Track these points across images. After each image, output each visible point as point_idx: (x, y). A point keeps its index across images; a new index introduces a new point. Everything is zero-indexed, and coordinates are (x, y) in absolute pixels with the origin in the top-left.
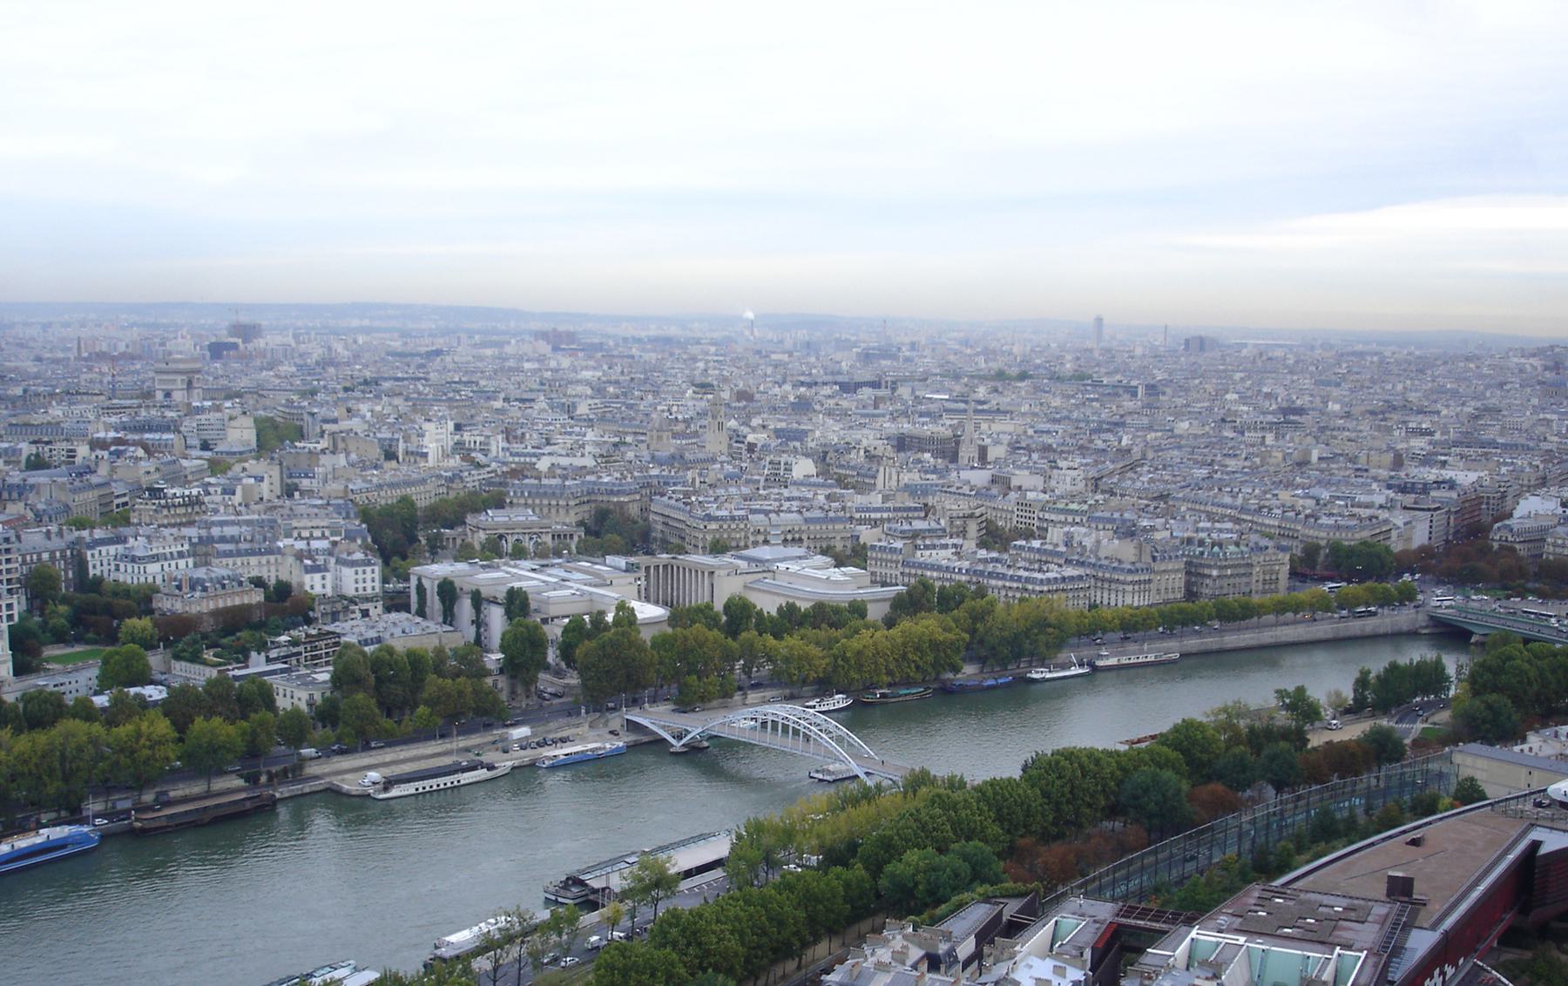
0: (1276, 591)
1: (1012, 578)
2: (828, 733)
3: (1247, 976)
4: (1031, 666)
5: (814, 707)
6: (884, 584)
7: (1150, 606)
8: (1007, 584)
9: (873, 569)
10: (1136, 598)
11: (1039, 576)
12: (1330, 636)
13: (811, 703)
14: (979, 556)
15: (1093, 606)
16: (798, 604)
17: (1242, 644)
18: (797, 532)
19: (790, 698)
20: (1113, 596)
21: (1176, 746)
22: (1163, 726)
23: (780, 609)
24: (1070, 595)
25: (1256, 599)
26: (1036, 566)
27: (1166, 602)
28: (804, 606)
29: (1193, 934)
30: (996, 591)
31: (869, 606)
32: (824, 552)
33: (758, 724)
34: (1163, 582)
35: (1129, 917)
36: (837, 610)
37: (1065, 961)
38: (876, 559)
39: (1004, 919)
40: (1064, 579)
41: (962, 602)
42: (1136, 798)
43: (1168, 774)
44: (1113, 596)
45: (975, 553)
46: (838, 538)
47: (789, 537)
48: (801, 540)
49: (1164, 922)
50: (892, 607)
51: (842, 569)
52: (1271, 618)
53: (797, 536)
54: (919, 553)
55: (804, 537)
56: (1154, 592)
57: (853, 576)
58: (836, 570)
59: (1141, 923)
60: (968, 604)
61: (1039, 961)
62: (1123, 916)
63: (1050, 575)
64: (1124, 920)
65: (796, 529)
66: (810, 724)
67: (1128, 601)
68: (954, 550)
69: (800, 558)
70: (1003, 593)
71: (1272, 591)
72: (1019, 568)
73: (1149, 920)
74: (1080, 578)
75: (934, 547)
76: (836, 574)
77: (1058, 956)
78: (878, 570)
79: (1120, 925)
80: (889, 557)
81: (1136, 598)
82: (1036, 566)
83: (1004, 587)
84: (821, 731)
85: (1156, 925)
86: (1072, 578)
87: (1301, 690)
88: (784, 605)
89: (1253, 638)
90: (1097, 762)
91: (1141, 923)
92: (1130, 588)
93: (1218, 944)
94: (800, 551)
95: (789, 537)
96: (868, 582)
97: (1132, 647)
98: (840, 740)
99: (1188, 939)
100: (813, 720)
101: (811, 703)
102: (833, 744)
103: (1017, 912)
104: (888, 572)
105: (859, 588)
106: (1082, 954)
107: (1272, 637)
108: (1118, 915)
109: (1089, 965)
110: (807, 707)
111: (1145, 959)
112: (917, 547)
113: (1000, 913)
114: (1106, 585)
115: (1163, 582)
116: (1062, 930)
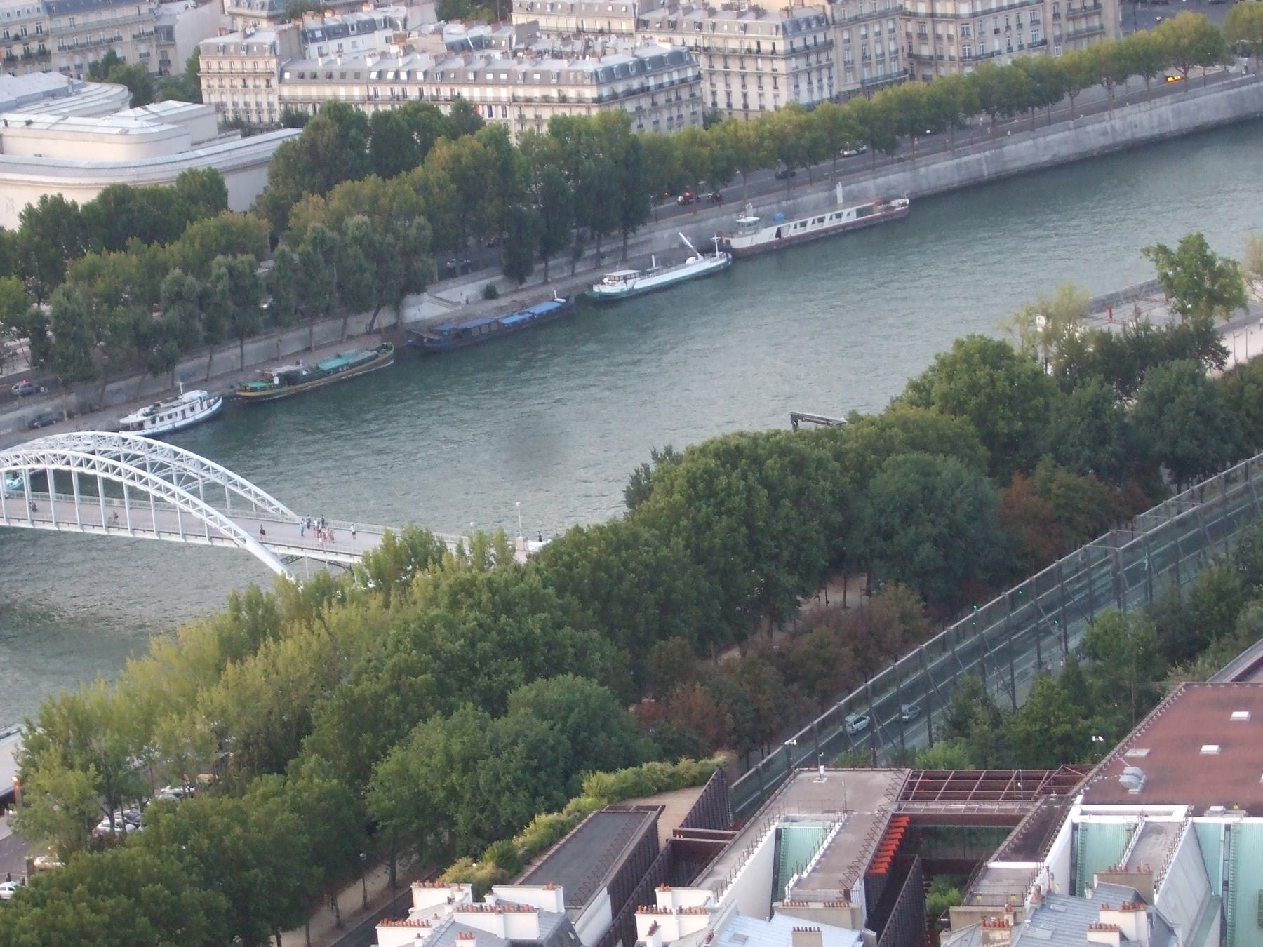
0: (1101, 31)
1: (526, 79)
2: (185, 479)
3: (1200, 889)
4: (598, 267)
5: (140, 426)
6: (248, 130)
7: (837, 99)
8: (521, 92)
9: (215, 98)
10: (803, 86)
11: (589, 65)
12: (1224, 114)
13: (133, 418)
14: (449, 39)
15: (711, 119)
16: (68, 198)
17: (1045, 158)
18: (33, 37)
19: (84, 413)
20: (752, 89)
21: (954, 405)
22: (919, 365)
23: (30, 216)
24: (661, 99)
25: (1060, 55)
26: (578, 45)
27: (868, 88)
28: (81, 196)
29: (1075, 814)
30: (497, 112)
31: (230, 183)
32: (100, 73)
33: (26, 480)
34: (857, 41)
35: (930, 799)
36: (155, 196)
37: (815, 916)
38: (220, 75)
39: (663, 844)
40: (641, 66)
41: (427, 146)
42: (888, 536)
43: (949, 466)
44: (752, 89)
45: (439, 32)
46: (127, 38)
47: (18, 50)
48: (44, 55)
49: (1009, 798)
50: (274, 176)
51: (152, 107)
52: (1097, 92)
53: (34, 47)
54: (313, 48)
55: (51, 45)
56: (838, 69)
57: (176, 120)
58: (139, 110)
59: (959, 807)
60: (442, 150)
61: (762, 924)
62: (918, 798)
63: (613, 60)
64: (920, 808)
65: (31, 29)
66: (143, 467)
67: (785, 96)
68: (389, 32)
69: (52, 95)
70: (513, 113)
71: (1091, 33)
72: (541, 54)
73: (976, 798)
74: (677, 59)
75: (342, 31)
76: (135, 119)
77: (798, 906)
78: (227, 99)
79: (914, 819)
80: (249, 66)
81: (803, 86)
82: (578, 45)
83: (515, 99)
84: (168, 478)
85: (992, 807)
86: (659, 63)
87: (1196, 246)
88: (36, 206)
89: (1065, 142)
90: (799, 466)
91: (959, 807)
92: (781, 66)
93: (1131, 829)
94: (55, 80)
95: (18, 50)
96: (214, 132)
97: (813, 196)
98: (213, 494)
99: (1065, 832)
100: (149, 457)
101: (133, 418)
102: (202, 504)
103: (687, 822)
104: (251, 99)
105: (197, 144)
106: (847, 895)
107: (1105, 133)
108: (906, 797)
109: (863, 917)
110: (127, 428)
111: (986, 887)
112: (306, 37)
113: (653, 830)
114: (734, 66)
115: (857, 41)
116: (792, 856)
